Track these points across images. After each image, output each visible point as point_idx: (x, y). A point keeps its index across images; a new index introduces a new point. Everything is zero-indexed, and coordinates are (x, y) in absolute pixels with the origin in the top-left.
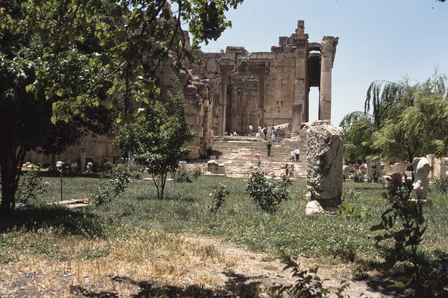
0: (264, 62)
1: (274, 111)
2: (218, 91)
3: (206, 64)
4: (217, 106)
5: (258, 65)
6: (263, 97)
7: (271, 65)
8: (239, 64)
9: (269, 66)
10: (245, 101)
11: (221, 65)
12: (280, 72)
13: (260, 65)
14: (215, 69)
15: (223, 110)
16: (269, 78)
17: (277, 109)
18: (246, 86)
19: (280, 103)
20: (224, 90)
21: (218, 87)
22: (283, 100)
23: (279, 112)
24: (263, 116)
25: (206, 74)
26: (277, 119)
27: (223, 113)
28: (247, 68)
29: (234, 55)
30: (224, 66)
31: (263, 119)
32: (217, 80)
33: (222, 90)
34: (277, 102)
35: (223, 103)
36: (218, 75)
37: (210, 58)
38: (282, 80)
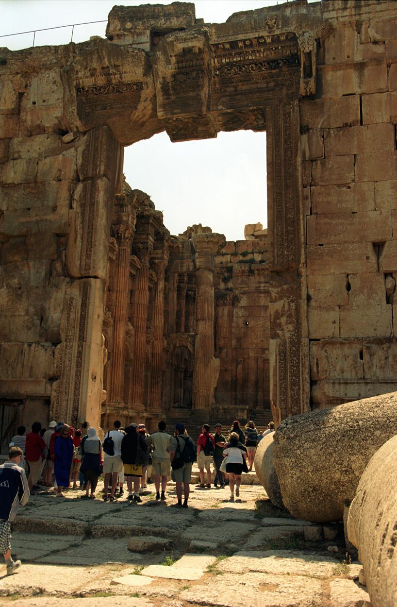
0: (293, 38)
1: (360, 299)
2: (63, 210)
3: (21, 96)
4: (57, 286)
5: (258, 64)
6: (295, 222)
7: (329, 58)
8: (166, 69)
9: (321, 61)
10: (241, 322)
11: (79, 89)
12: (382, 85)
13: (273, 64)
14: (58, 113)
15: (85, 305)
16: (320, 122)
18: (243, 282)
20: (93, 204)
21: (64, 194)
25: (15, 141)
27: (84, 318)
28: (205, 92)
29: (146, 38)
30: (96, 88)
31: (296, 343)
32: (65, 160)
33: (83, 206)
34: (378, 247)
35: (88, 267)
36: (68, 138)
37: (35, 70)
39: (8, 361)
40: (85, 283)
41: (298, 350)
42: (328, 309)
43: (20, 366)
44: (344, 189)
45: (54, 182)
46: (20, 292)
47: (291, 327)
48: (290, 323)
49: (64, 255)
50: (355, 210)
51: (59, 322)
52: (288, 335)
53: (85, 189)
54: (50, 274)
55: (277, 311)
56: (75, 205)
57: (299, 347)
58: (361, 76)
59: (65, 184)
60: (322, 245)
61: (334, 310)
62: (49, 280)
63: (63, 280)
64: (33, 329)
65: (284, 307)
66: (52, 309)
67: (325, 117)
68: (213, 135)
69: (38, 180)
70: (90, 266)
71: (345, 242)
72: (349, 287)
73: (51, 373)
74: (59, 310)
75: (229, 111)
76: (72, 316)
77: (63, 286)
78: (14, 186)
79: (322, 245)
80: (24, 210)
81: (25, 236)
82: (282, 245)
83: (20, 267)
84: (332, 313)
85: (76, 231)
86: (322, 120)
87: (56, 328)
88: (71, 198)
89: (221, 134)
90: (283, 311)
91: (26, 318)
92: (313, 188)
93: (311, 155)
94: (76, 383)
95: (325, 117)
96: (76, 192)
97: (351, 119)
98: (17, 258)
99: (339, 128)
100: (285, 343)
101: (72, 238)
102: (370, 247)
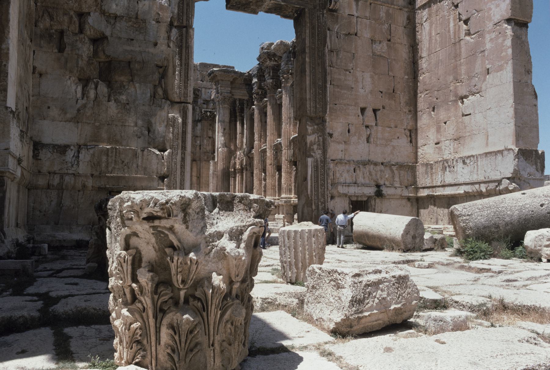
1: (354, 139)
12: (367, 14)
15: (184, 123)
17: (365, 133)
19: (369, 113)
21: (163, 34)
22: (378, 106)
23: (368, 141)
24: (325, 152)
26: (365, 163)
31: (324, 161)
33: (180, 47)
34: (363, 110)
38: (373, 41)
39: (123, 162)
40: (184, 107)
41: (324, 166)
42: (339, 143)
43: (135, 165)
44: (348, 73)
45: (154, 22)
46: (128, 107)
47: (320, 152)
48: (319, 149)
49: (163, 82)
50: (353, 86)
51: (164, 134)
52: (318, 156)
53: (181, 35)
54: (154, 96)
55: (311, 141)
56: (171, 45)
57: (325, 164)
58: (357, 5)
59: (164, 28)
60: (336, 104)
61: (342, 143)
62: (154, 100)
63: (165, 102)
64: (142, 138)
65: (315, 139)
66: (158, 124)
67: (339, 25)
68: (255, 12)
69: (139, 17)
70: (187, 94)
71: (348, 105)
72: (349, 131)
73: (162, 173)
74: (163, 125)
75: (283, 3)
76: (176, 131)
77: (166, 108)
78: (116, 17)
79: (336, 104)
80: (128, 39)
81: (129, 62)
82: (315, 101)
83: (126, 87)
84: (341, 145)
85: (174, 67)
86: (337, 27)
87: (162, 139)
88: (169, 38)
89: (261, 14)
90: (315, 141)
91: (135, 128)
92: (332, 68)
93: (331, 47)
94: (181, 181)
95: (339, 25)
96: (172, 34)
97: (352, 31)
98: (122, 78)
99: (346, 35)
100: (317, 161)
101: (170, 70)
102: (359, 110)
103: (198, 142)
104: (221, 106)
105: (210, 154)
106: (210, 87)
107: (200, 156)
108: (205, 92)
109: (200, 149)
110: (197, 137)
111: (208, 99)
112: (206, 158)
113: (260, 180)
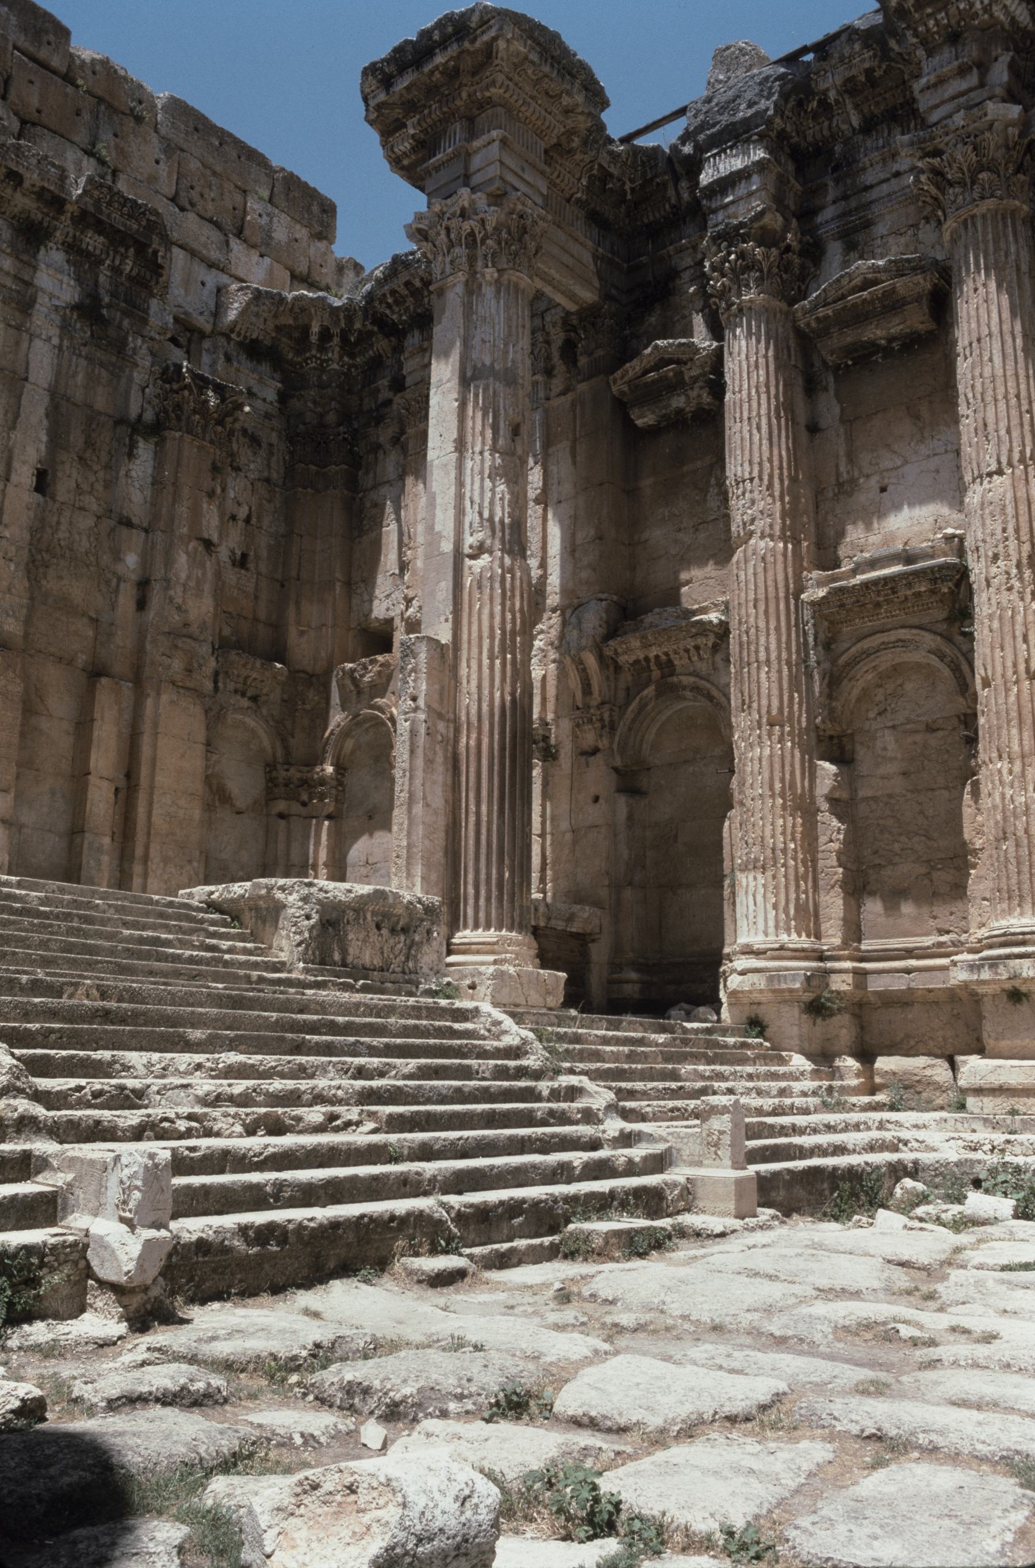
103: (131, 560)
104: (490, 273)
105: (205, 649)
106: (214, 255)
107: (140, 650)
108: (187, 283)
109: (141, 605)
110: (128, 523)
111: (204, 323)
112: (177, 665)
113: (804, 808)
